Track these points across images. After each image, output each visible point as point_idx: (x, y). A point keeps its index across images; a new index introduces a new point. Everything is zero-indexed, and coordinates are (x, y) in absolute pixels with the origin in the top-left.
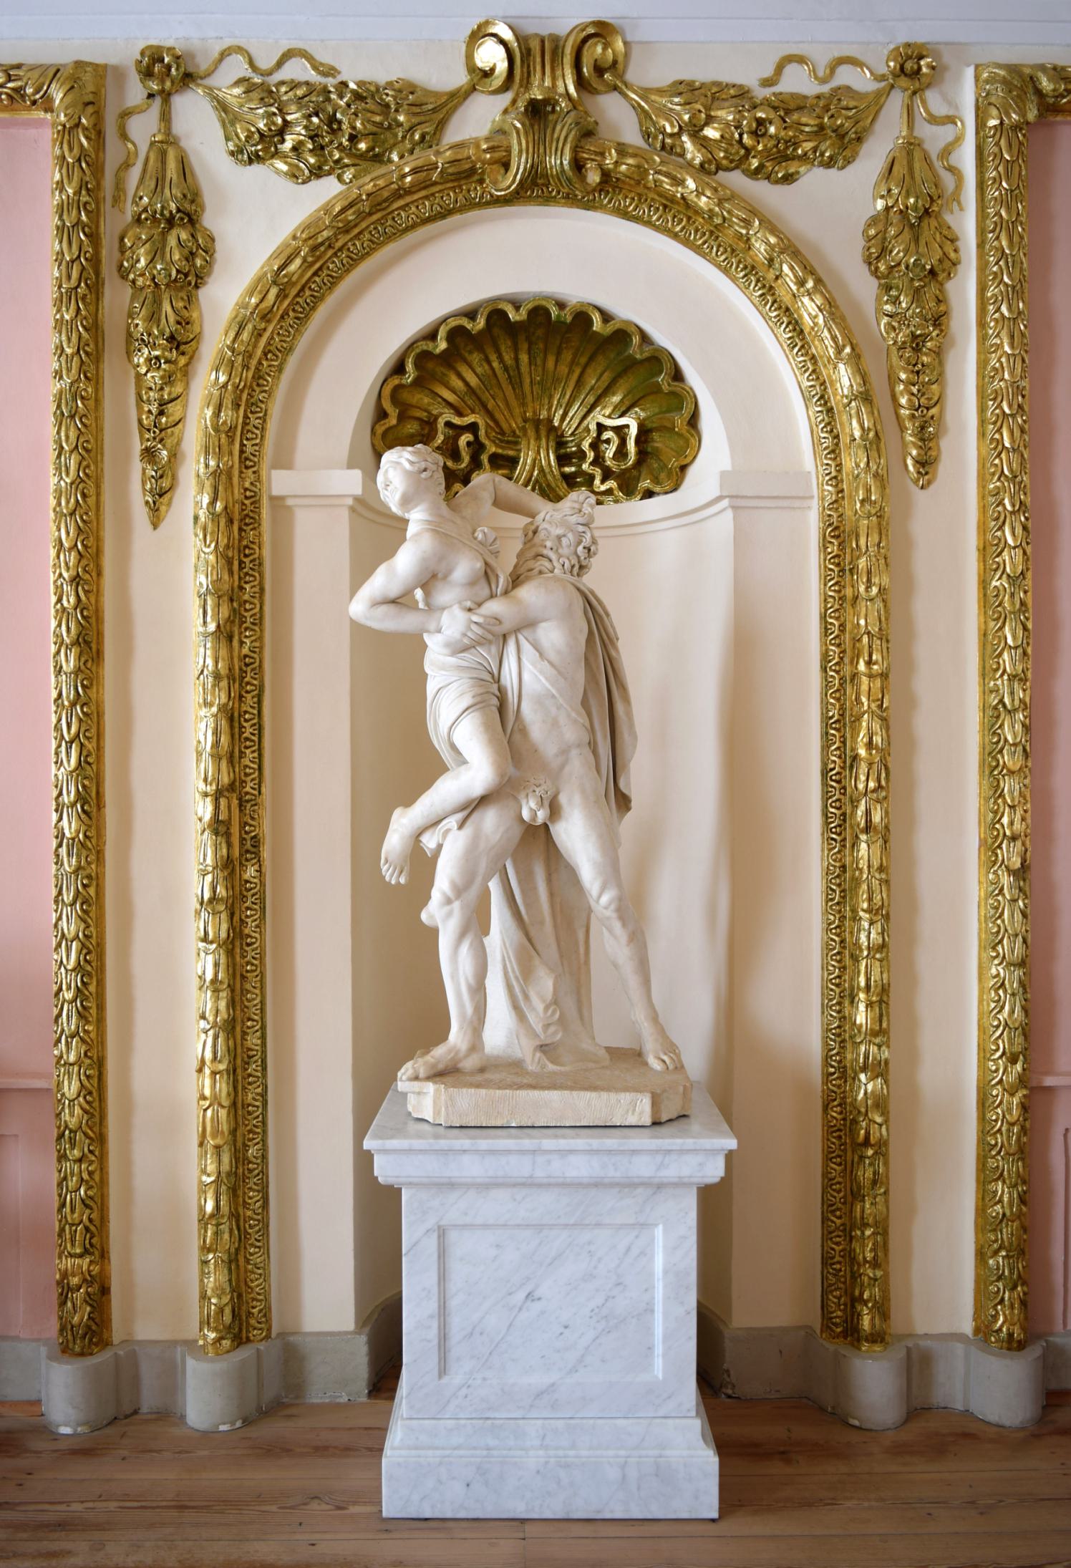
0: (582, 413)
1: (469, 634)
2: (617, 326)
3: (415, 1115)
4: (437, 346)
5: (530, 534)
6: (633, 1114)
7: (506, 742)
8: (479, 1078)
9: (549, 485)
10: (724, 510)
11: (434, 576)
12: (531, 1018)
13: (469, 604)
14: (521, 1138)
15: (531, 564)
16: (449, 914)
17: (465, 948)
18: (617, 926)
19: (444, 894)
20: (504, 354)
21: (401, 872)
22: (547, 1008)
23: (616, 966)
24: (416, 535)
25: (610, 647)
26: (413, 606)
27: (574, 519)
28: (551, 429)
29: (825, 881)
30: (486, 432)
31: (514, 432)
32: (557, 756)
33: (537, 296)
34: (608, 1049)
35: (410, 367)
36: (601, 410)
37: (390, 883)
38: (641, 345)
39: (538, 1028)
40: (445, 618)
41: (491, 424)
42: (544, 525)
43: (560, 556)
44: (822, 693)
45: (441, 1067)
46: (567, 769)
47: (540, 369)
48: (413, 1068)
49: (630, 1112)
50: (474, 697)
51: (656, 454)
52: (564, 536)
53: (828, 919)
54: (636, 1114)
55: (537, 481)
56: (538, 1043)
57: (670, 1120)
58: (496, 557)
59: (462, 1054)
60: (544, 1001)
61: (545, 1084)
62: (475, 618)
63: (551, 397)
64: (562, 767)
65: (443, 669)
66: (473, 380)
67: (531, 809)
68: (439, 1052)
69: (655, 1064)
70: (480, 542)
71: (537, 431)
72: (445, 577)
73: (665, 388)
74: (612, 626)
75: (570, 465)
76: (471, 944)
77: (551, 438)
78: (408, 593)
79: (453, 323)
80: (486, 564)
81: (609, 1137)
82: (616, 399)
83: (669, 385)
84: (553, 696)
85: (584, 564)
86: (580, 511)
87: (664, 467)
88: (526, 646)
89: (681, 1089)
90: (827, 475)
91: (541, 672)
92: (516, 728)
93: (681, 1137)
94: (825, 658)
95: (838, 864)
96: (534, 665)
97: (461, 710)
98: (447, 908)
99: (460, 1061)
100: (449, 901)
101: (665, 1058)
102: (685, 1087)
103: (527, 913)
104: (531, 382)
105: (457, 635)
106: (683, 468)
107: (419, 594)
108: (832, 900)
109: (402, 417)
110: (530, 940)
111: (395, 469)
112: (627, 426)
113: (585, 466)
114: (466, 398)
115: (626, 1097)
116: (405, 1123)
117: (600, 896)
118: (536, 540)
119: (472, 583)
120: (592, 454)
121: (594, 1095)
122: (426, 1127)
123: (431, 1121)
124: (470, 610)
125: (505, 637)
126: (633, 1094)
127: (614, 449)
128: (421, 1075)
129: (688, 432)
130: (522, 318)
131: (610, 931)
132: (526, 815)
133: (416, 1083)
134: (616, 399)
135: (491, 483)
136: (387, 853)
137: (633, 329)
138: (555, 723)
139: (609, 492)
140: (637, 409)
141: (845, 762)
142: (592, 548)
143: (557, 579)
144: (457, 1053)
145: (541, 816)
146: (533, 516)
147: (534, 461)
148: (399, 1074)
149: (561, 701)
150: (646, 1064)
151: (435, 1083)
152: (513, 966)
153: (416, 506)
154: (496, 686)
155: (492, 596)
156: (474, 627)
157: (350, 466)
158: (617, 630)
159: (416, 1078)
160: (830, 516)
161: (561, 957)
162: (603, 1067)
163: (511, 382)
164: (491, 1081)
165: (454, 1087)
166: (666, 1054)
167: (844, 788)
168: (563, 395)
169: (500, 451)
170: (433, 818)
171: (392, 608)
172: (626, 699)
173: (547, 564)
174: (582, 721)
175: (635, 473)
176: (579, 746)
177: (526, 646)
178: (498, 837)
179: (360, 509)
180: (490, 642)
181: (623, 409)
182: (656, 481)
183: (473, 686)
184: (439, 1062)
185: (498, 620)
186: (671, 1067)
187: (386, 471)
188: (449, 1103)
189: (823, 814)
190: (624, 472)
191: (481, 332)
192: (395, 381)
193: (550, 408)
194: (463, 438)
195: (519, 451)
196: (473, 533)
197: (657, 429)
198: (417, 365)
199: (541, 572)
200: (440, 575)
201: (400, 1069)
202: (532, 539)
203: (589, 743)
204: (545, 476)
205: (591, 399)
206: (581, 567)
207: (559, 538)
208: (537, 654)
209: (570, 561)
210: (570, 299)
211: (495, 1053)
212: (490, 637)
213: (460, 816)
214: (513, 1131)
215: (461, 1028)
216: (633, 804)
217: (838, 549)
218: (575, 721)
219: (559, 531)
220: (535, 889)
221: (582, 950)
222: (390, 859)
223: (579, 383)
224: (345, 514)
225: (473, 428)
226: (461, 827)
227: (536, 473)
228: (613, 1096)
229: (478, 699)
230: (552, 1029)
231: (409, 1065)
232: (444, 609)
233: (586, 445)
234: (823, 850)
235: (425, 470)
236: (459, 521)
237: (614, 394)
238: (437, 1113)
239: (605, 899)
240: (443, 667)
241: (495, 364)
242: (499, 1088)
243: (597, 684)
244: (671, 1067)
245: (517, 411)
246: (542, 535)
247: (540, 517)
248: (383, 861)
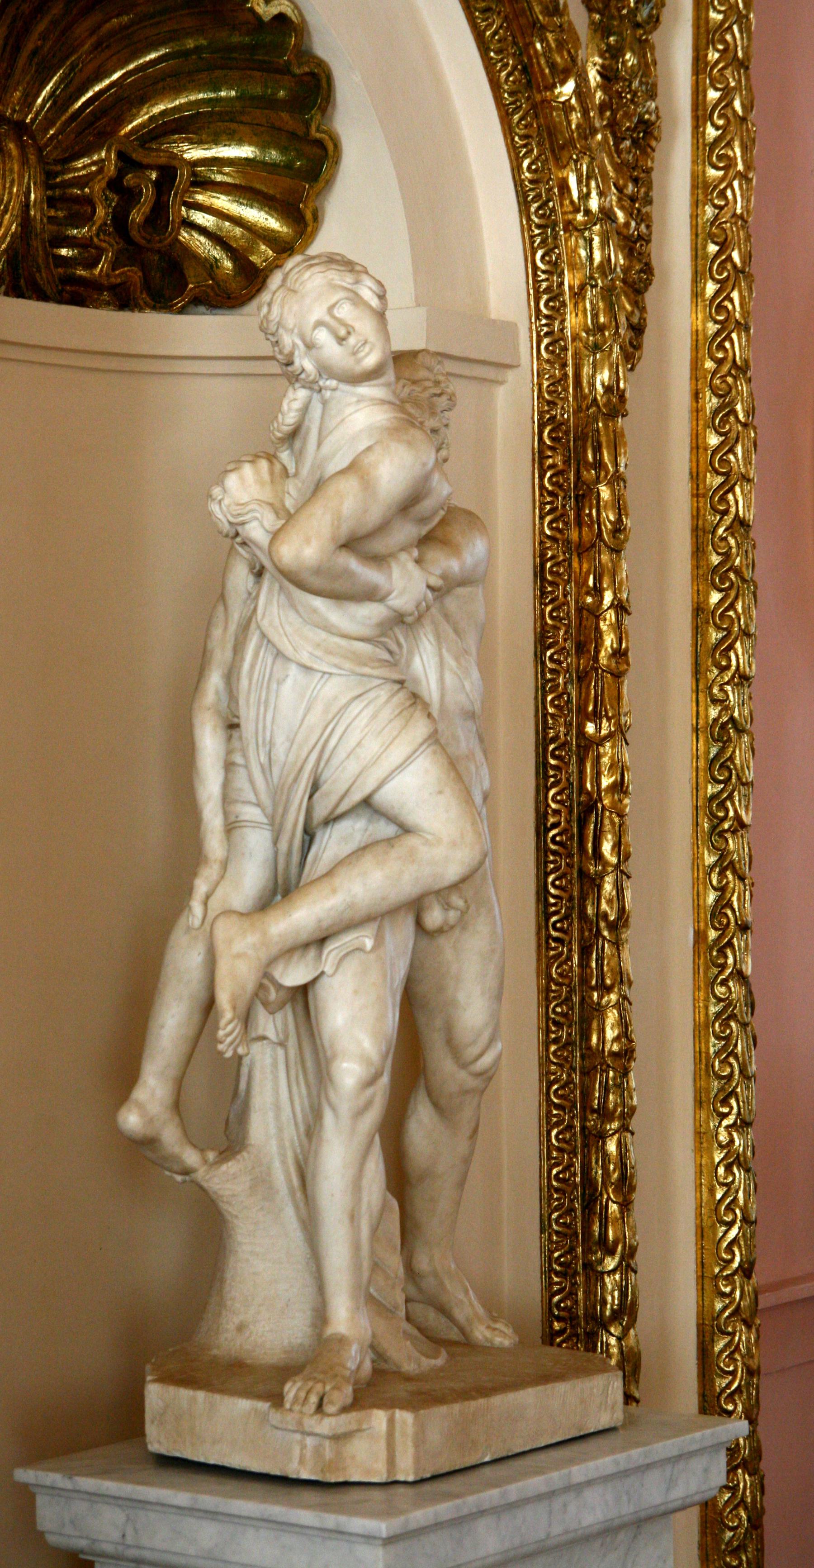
29: (542, 1010)
44: (536, 698)
53: (549, 1073)
90: (547, 334)
94: (542, 641)
95: (566, 981)
108: (556, 1041)
141: (570, 812)
160: (549, 403)
167: (570, 856)
189: (538, 901)
217: (564, 462)
234: (539, 960)
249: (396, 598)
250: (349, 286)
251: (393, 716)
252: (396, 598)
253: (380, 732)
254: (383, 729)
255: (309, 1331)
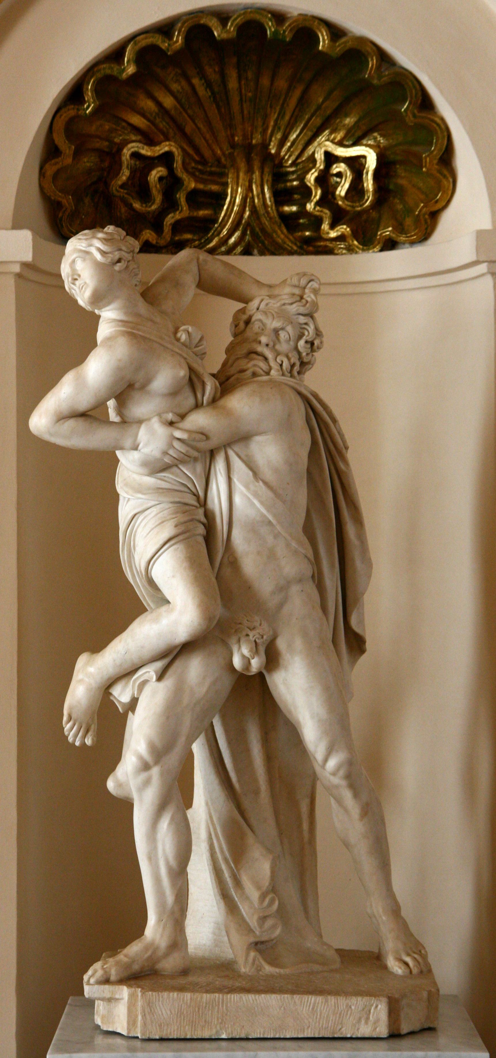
0: (306, 138)
1: (171, 452)
2: (349, 45)
3: (105, 1028)
4: (124, 70)
5: (242, 325)
6: (366, 1023)
7: (214, 579)
8: (182, 981)
9: (263, 230)
10: (483, 275)
11: (131, 386)
12: (244, 909)
13: (170, 416)
14: (233, 1050)
15: (243, 364)
16: (147, 782)
17: (165, 824)
18: (347, 795)
19: (141, 758)
20: (207, 68)
21: (87, 731)
22: (263, 897)
23: (347, 845)
24: (109, 339)
25: (338, 458)
26: (105, 421)
27: (294, 309)
28: (267, 157)
30: (184, 163)
31: (219, 161)
32: (273, 593)
33: (247, 9)
34: (339, 952)
35: (89, 94)
36: (331, 133)
37: (73, 744)
38: (379, 67)
39: (253, 922)
40: (143, 434)
41: (191, 151)
42: (258, 316)
43: (278, 354)
45: (136, 967)
46: (286, 609)
47: (252, 84)
48: (102, 968)
49: (363, 1021)
50: (176, 526)
51: (401, 192)
52: (283, 329)
54: (370, 1024)
55: (248, 224)
56: (252, 940)
57: (412, 1033)
58: (202, 359)
59: (160, 953)
60: (258, 888)
61: (262, 988)
62: (178, 434)
63: (266, 118)
64: (281, 606)
65: (140, 492)
66: (168, 102)
67: (243, 657)
68: (134, 949)
69: (396, 968)
70: (184, 344)
71: (249, 162)
72: (144, 387)
73: (410, 120)
74: (340, 433)
75: (290, 202)
76: (172, 819)
77: (267, 170)
78: (100, 406)
79: (144, 41)
80: (191, 369)
81: (337, 1049)
82: (349, 121)
83: (414, 116)
84: (270, 523)
85: (305, 360)
86: (302, 298)
87: (409, 211)
88: (237, 464)
89: (425, 994)
91: (256, 495)
92: (226, 561)
93: (422, 1050)
96: (247, 487)
97: (161, 542)
98: (144, 775)
99: (158, 960)
100: (146, 767)
101: (408, 959)
102: (430, 992)
103: (239, 781)
104: (241, 100)
105: (157, 454)
106: (434, 216)
107: (111, 404)
109: (77, 154)
110: (242, 812)
111: (84, 260)
112: (364, 157)
113: (310, 207)
114: (158, 121)
115: (357, 1003)
116: (92, 1038)
117: (326, 760)
118: (249, 333)
119: (174, 393)
120: (319, 192)
121: (320, 999)
122: (119, 1041)
123: (125, 1033)
124: (171, 424)
125: (212, 454)
126: (366, 999)
127: (347, 186)
128: (113, 978)
129: (440, 172)
130: (230, 36)
131: (339, 802)
132: (237, 662)
133: (107, 987)
134: (349, 121)
135: (195, 263)
136: (71, 708)
137: (369, 48)
138: (272, 555)
139: (341, 238)
140: (376, 134)
142: (316, 342)
143: (273, 383)
144: (154, 952)
145: (256, 664)
146: (246, 300)
147: (244, 200)
148: (86, 977)
149: (278, 527)
150: (385, 967)
151: (129, 986)
152: (221, 845)
153: (109, 304)
154: (201, 511)
155: (198, 406)
156: (177, 444)
157: (16, 226)
158: (347, 437)
159: (106, 981)
161: (281, 833)
162: (331, 971)
163: (215, 98)
164: (197, 984)
165: (153, 990)
166: (408, 955)
168: (281, 115)
169: (201, 186)
170: (127, 667)
171: (80, 421)
172: (358, 520)
173: (262, 364)
174: (303, 551)
175: (374, 214)
176: (300, 581)
177: (237, 464)
178: (205, 690)
179: (30, 275)
180: (196, 459)
181: (359, 133)
182: (400, 228)
183: (176, 513)
184: (133, 962)
185: (205, 435)
186: (415, 971)
187: (74, 261)
188: (147, 1010)
190: (360, 214)
191: (179, 53)
192: (71, 112)
193: (265, 131)
194: (154, 173)
195: (226, 185)
196: (176, 332)
197: (401, 162)
198: (97, 91)
199: (254, 375)
200: (137, 385)
201: (86, 971)
202: (244, 330)
203: (313, 577)
204: (258, 218)
205: (317, 121)
206: (303, 364)
207: (276, 332)
208: (251, 473)
209: (289, 359)
210: (290, 10)
211: (200, 953)
212: (195, 454)
213: (159, 665)
214: (224, 1044)
215: (159, 920)
216: (368, 645)
218: (296, 552)
219: (276, 324)
220: (247, 750)
221: (305, 826)
222: (74, 716)
223: (302, 102)
224: (11, 282)
225: (167, 159)
226: (160, 678)
227: (247, 213)
228: (342, 1001)
229: (182, 528)
230: (269, 923)
231: (98, 966)
232: (140, 422)
233: (311, 177)
235: (119, 261)
236: (158, 319)
237: (347, 115)
238: (132, 1022)
239: (332, 763)
240: (139, 489)
241: (196, 81)
242: (207, 992)
243: (323, 503)
244: (415, 971)
245: (222, 135)
246: (256, 326)
247: (254, 304)
248: (65, 718)
249: (143, 447)
250: (84, 249)
251: (154, 526)
252: (143, 447)
253: (146, 537)
254: (148, 534)
255: (211, 936)
